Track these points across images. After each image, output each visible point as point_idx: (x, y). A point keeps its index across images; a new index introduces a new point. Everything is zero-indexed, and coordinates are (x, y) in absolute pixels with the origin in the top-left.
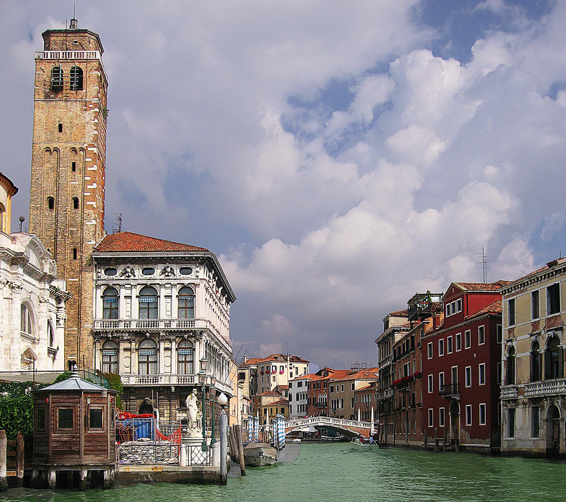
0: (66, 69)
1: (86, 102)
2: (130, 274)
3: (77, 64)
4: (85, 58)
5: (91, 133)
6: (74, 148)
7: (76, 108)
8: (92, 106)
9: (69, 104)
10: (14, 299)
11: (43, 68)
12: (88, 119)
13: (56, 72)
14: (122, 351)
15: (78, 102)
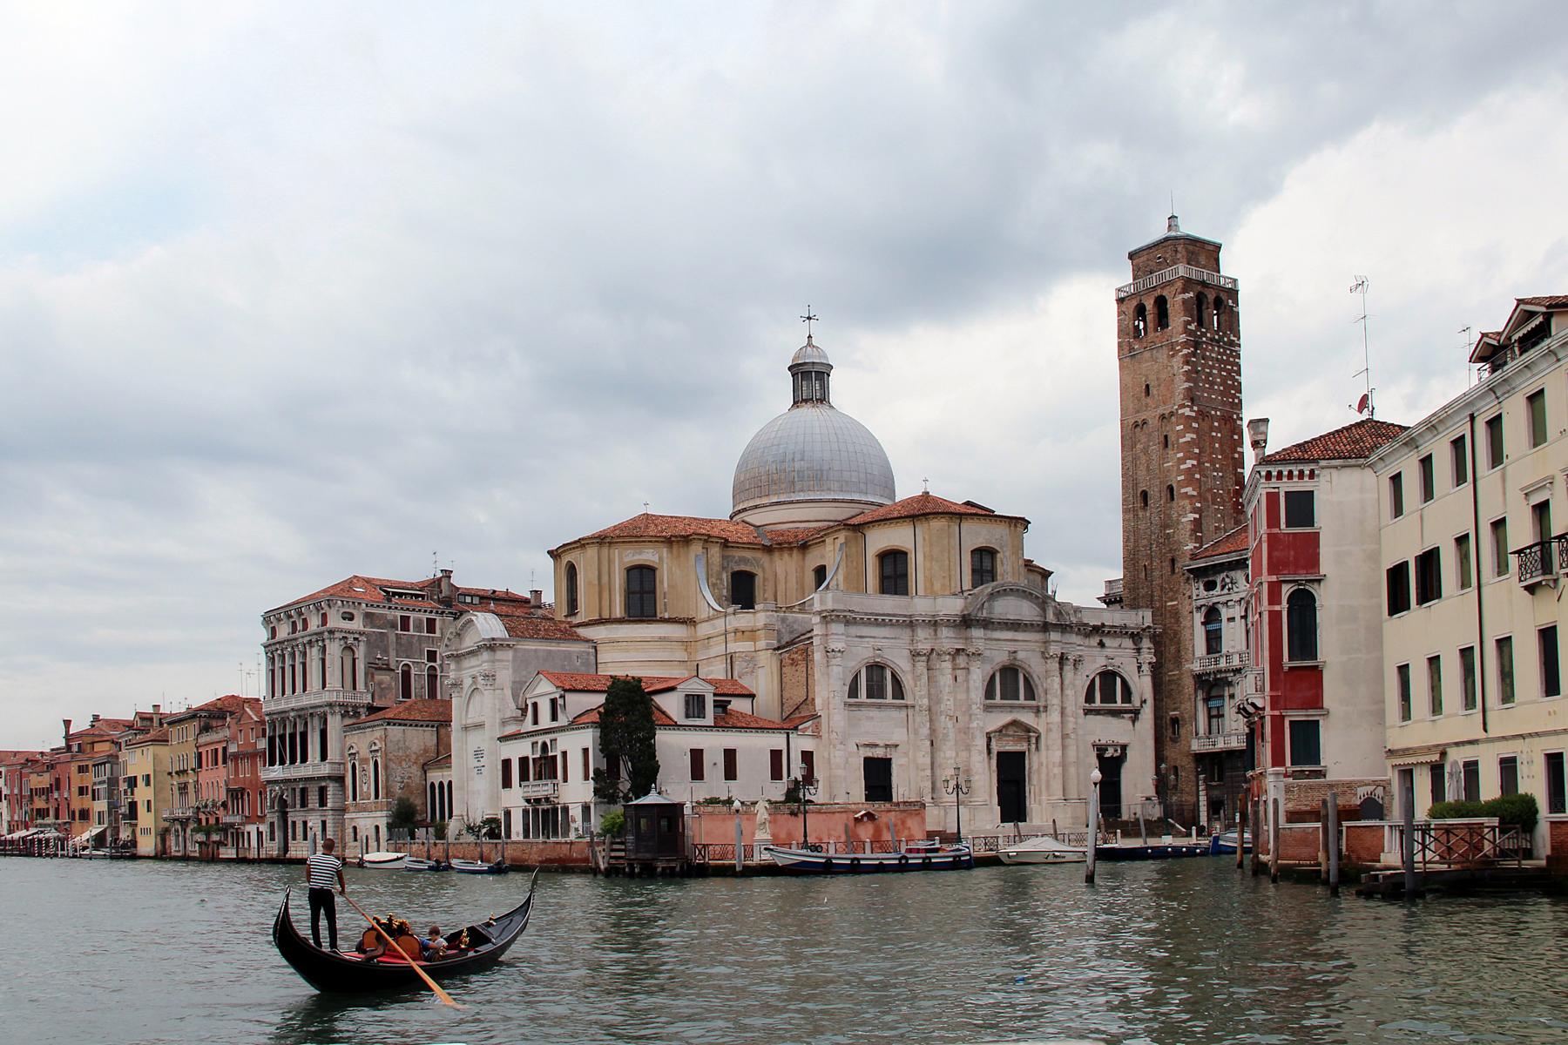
2: (1230, 585)
10: (971, 668)
14: (1227, 699)
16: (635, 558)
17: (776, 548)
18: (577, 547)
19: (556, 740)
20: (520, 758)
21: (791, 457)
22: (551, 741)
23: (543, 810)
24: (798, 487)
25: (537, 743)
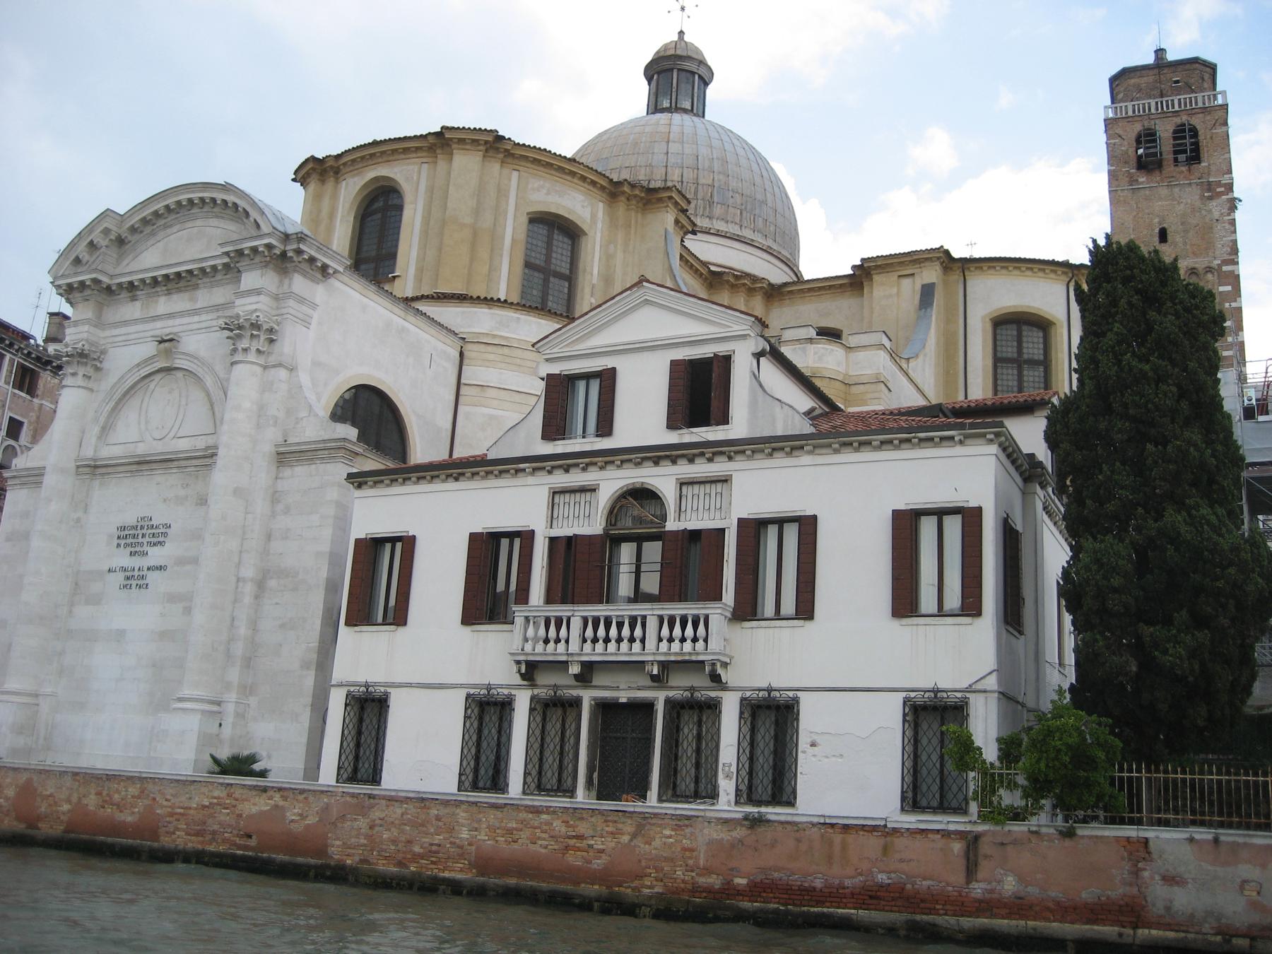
0: (1165, 130)
1: (1209, 183)
3: (1184, 118)
4: (1200, 105)
5: (1224, 239)
6: (1194, 268)
7: (1190, 196)
8: (1223, 189)
9: (1176, 190)
11: (1121, 132)
12: (1216, 214)
13: (1147, 137)
15: (1194, 186)
16: (550, 199)
17: (728, 281)
18: (418, 149)
19: (725, 480)
20: (473, 537)
21: (707, 164)
22: (682, 484)
23: (606, 709)
24: (718, 210)
25: (592, 490)
